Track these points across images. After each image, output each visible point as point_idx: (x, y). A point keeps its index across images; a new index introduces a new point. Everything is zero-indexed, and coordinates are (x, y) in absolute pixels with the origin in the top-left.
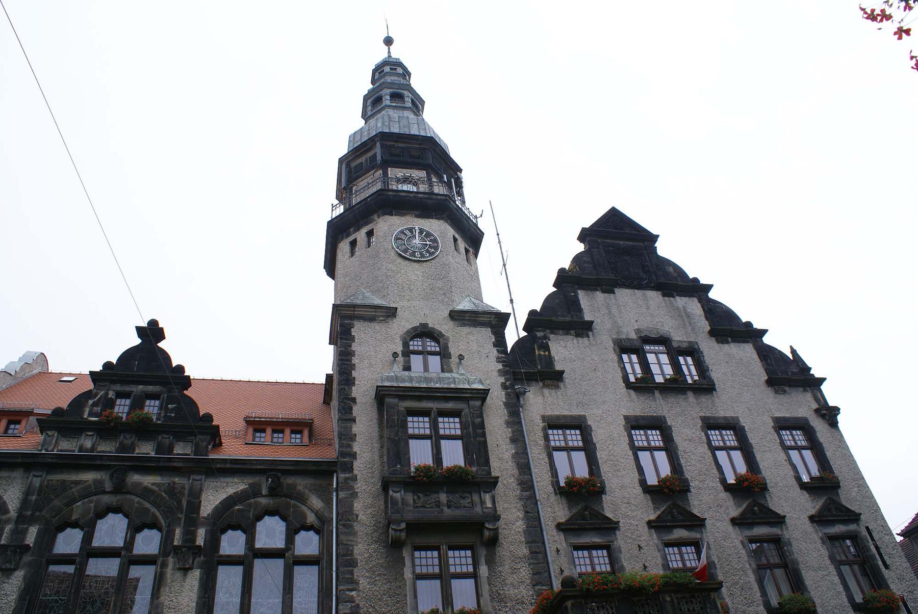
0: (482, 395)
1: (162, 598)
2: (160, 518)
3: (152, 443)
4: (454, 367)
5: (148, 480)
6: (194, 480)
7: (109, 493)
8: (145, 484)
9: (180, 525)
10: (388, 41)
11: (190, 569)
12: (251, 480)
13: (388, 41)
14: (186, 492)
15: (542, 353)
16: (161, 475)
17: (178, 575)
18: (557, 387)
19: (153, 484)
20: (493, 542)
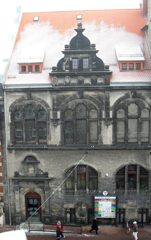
1: (102, 134)
3: (89, 79)
5: (91, 94)
6: (106, 93)
7: (79, 99)
8: (90, 95)
9: (104, 110)
11: (109, 125)
12: (125, 92)
14: (104, 98)
16: (95, 92)
17: (105, 127)
19: (93, 95)
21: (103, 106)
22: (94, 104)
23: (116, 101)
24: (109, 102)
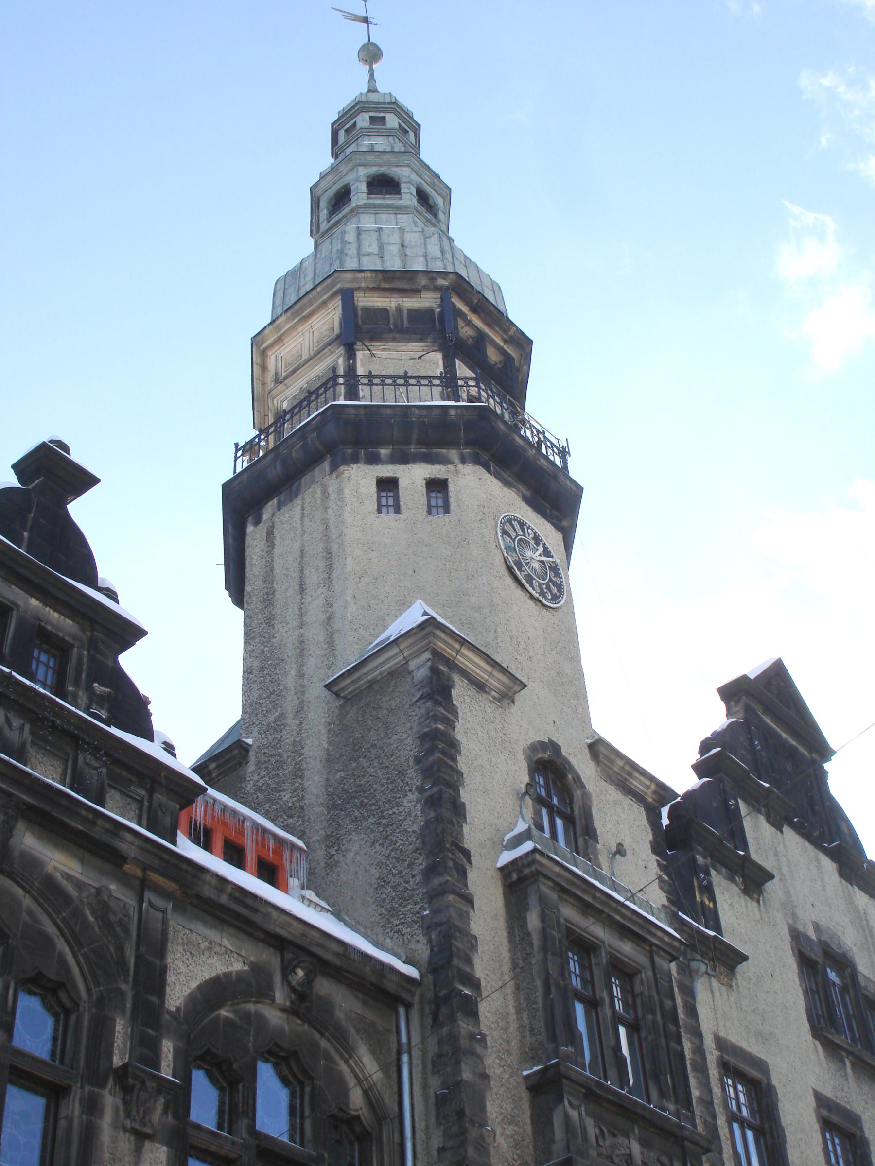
2: (76, 971)
4: (603, 859)
5: (60, 862)
6: (151, 904)
8: (50, 869)
9: (123, 1011)
10: (371, 54)
13: (371, 54)
15: (707, 902)
17: (125, 1143)
19: (68, 877)
21: (124, 987)
22: (62, 946)
23: (200, 987)
24: (164, 970)
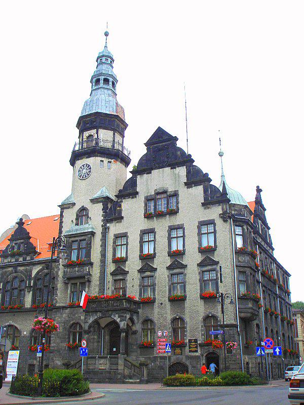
0: (93, 234)
18: (121, 222)
20: (89, 281)
